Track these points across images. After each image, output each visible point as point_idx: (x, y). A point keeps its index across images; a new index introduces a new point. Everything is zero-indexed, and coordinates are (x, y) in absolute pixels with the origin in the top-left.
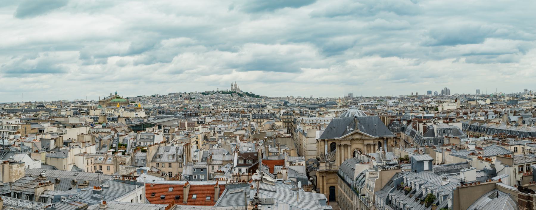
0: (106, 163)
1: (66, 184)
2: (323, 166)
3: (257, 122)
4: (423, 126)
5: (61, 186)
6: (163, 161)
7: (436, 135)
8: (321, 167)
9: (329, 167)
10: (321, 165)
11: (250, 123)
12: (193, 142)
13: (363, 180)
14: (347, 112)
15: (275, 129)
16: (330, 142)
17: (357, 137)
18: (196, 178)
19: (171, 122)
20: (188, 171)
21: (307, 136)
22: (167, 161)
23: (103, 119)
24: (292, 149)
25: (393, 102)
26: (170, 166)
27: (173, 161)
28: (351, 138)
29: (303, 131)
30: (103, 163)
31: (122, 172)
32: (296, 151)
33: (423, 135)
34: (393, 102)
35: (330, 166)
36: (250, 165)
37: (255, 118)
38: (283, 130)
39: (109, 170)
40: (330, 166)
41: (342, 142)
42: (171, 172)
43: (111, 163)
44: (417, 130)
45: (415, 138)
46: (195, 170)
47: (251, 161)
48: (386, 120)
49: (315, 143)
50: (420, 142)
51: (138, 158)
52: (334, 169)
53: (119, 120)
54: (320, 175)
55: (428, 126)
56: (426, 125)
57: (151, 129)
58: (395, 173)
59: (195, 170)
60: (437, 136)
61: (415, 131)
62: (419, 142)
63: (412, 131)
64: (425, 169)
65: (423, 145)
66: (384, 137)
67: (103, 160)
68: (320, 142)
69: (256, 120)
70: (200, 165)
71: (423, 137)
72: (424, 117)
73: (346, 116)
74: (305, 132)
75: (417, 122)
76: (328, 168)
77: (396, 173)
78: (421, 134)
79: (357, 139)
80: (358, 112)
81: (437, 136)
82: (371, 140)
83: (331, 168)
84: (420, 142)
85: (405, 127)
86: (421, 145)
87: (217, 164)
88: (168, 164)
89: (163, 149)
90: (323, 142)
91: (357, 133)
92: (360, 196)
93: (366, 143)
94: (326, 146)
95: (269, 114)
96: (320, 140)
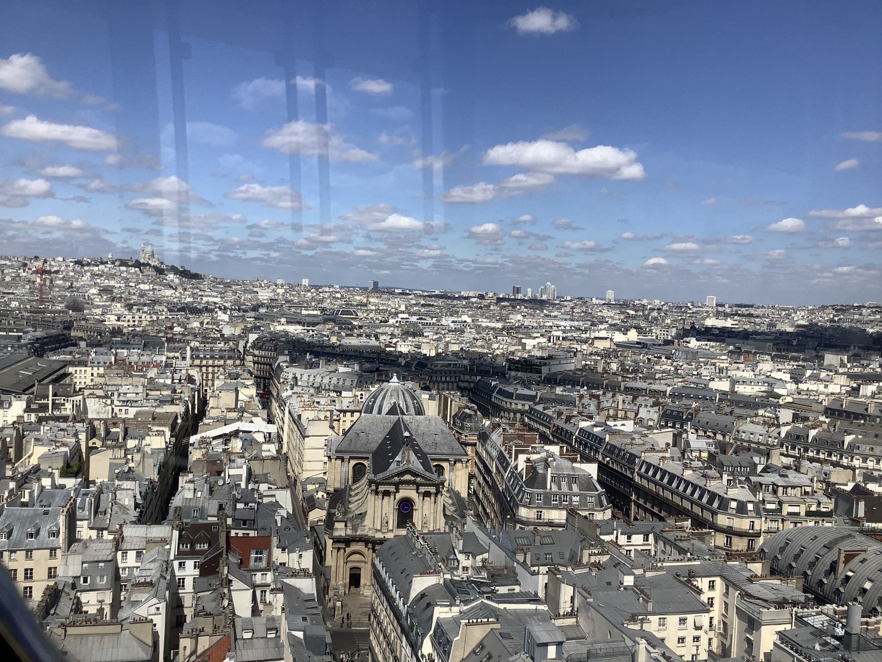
2: (341, 529)
7: (548, 487)
8: (337, 529)
10: (338, 525)
16: (353, 462)
17: (408, 477)
18: (89, 582)
20: (71, 567)
21: (307, 434)
25: (453, 322)
29: (299, 416)
33: (524, 480)
34: (453, 322)
35: (355, 528)
40: (355, 528)
42: (31, 570)
44: (510, 457)
49: (321, 447)
52: (362, 533)
60: (551, 489)
61: (507, 456)
64: (549, 657)
68: (333, 461)
72: (517, 394)
74: (304, 420)
76: (349, 532)
77: (491, 629)
79: (408, 482)
81: (551, 489)
87: (133, 548)
91: (408, 472)
93: (422, 489)
95: (225, 350)
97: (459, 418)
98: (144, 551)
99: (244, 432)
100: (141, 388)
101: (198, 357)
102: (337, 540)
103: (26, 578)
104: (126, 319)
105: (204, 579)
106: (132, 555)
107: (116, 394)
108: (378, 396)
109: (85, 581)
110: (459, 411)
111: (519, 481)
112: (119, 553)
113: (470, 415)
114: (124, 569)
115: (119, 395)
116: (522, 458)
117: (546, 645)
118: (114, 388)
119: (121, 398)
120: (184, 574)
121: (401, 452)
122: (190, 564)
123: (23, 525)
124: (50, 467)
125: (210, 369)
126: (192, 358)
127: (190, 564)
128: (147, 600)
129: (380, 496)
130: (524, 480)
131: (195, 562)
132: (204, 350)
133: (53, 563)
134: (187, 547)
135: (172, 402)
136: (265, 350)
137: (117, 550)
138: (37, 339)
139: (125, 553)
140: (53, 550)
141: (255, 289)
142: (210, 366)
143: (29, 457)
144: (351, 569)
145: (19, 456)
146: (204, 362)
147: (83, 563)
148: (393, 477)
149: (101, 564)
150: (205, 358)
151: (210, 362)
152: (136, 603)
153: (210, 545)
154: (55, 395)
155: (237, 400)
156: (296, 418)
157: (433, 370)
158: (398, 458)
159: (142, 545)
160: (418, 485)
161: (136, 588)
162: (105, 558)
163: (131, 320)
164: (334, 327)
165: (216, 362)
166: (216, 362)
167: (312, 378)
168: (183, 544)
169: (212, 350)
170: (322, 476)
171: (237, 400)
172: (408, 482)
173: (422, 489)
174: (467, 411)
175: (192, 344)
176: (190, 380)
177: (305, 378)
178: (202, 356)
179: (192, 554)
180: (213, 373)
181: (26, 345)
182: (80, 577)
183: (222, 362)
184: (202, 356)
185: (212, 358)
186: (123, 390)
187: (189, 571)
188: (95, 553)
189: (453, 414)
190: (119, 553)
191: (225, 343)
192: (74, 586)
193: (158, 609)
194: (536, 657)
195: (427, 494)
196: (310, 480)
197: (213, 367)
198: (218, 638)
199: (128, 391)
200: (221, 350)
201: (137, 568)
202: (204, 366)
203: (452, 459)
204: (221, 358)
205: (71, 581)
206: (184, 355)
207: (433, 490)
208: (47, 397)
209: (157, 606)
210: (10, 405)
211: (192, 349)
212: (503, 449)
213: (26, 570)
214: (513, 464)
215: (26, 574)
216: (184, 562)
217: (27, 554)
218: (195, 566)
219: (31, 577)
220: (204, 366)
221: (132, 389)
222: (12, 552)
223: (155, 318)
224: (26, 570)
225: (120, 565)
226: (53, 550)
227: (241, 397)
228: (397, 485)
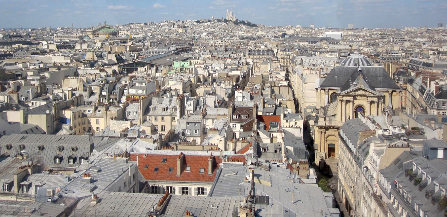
0: (95, 116)
1: (51, 151)
3: (253, 59)
4: (436, 86)
5: (46, 153)
6: (156, 114)
9: (329, 122)
11: (246, 61)
12: (187, 87)
13: (366, 151)
14: (349, 58)
15: (272, 72)
16: (331, 92)
19: (164, 59)
20: (182, 125)
22: (160, 114)
24: (290, 100)
26: (163, 118)
27: (166, 114)
28: (353, 93)
29: (302, 75)
30: (92, 116)
31: (113, 127)
32: (293, 102)
33: (434, 95)
36: (245, 121)
37: (251, 55)
38: (281, 73)
39: (99, 123)
40: (330, 121)
41: (344, 97)
42: (164, 126)
43: (101, 116)
44: (427, 87)
45: (424, 95)
46: (188, 125)
47: (246, 118)
48: (391, 67)
50: (431, 103)
51: (130, 111)
54: (319, 131)
55: (442, 86)
56: (438, 84)
57: (143, 69)
58: (403, 151)
59: (188, 125)
61: (424, 86)
62: (429, 103)
63: (422, 86)
65: (434, 107)
66: (389, 91)
68: (319, 91)
69: (251, 57)
71: (434, 98)
73: (346, 65)
75: (428, 79)
78: (432, 94)
79: (361, 95)
80: (361, 58)
82: (375, 97)
83: (331, 124)
84: (431, 103)
85: (414, 79)
86: (432, 106)
88: (161, 117)
89: (156, 100)
90: (322, 91)
91: (360, 89)
92: (362, 168)
93: (370, 99)
94: (326, 96)
95: (265, 51)
96: (320, 89)
97: (397, 75)
100: (222, 64)
102: (320, 128)
103: (162, 130)
104: (219, 43)
105: (246, 133)
108: (347, 60)
109: (188, 132)
110: (397, 71)
111: (431, 96)
113: (403, 72)
115: (212, 68)
116: (433, 83)
117: (436, 149)
119: (213, 69)
120: (236, 131)
121: (356, 80)
122: (238, 125)
127: (238, 125)
129: (344, 103)
130: (434, 95)
131: (241, 125)
135: (237, 70)
144: (329, 145)
145: (164, 85)
148: (351, 92)
151: (258, 57)
153: (248, 116)
156: (301, 76)
157: (383, 58)
158: (354, 83)
160: (367, 97)
163: (221, 43)
169: (259, 51)
170: (315, 105)
172: (361, 95)
173: (370, 99)
174: (401, 70)
176: (247, 64)
177: (307, 61)
179: (240, 121)
185: (259, 54)
187: (238, 129)
188: (193, 120)
189: (393, 73)
192: (184, 134)
194: (429, 157)
195: (372, 102)
196: (308, 108)
198: (247, 144)
202: (255, 59)
203: (390, 90)
205: (182, 131)
207: (376, 99)
212: (423, 84)
213: (162, 126)
214: (428, 89)
215: (162, 128)
216: (235, 125)
218: (241, 127)
219: (165, 130)
220: (255, 59)
221: (218, 65)
223: (232, 41)
224: (162, 126)
228: (355, 97)
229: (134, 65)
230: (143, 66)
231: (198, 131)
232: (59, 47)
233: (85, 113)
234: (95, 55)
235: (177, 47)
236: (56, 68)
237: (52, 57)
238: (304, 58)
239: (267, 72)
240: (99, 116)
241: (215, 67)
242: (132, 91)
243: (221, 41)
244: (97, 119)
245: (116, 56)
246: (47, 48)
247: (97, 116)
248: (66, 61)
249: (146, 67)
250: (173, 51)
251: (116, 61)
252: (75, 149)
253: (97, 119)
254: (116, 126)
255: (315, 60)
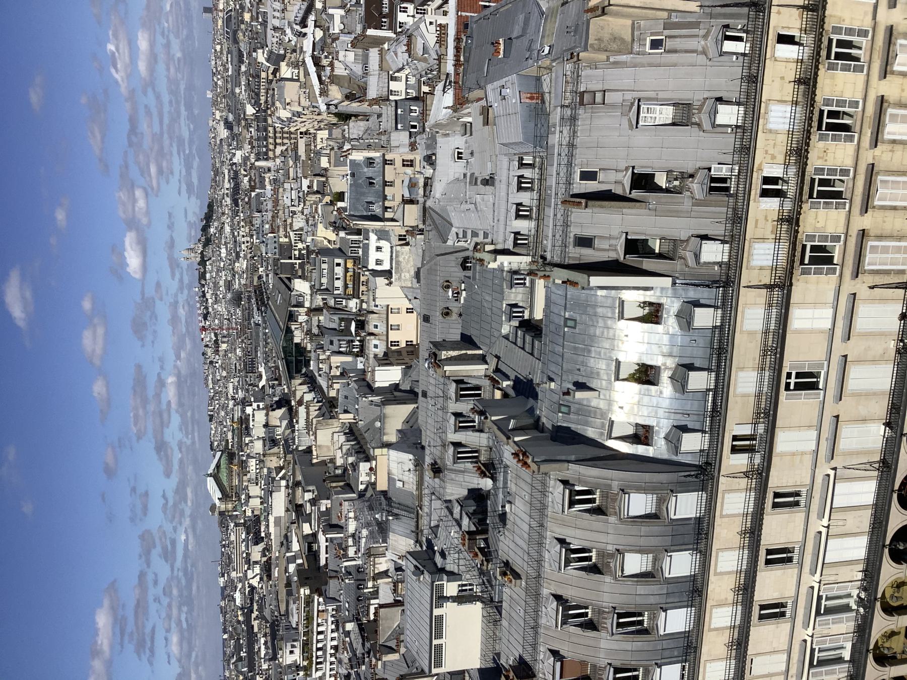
0: (385, 333)
18: (415, 124)
22: (381, 189)
23: (272, 458)
30: (385, 338)
39: (399, 325)
43: (385, 322)
53: (274, 424)
67: (379, 340)
70: (390, 121)
95: (258, 125)
98: (391, 72)
99: (314, 50)
101: (266, 153)
106: (394, 85)
107: (292, 209)
112: (392, 98)
114: (407, 93)
118: (287, 210)
119: (296, 203)
123: (363, 194)
124: (332, 213)
125: (278, 141)
126: (267, 159)
128: (423, 37)
131: (400, 11)
132: (258, 147)
133: (399, 163)
134: (385, 22)
136: (259, 89)
137: (388, 100)
138: (258, 309)
139: (391, 92)
140: (385, 162)
141: (218, 142)
142: (275, 141)
143: (329, 241)
146: (271, 147)
147: (396, 128)
149: (399, 111)
150: (266, 146)
151: (271, 141)
152: (425, 50)
154: (290, 258)
155: (291, 80)
159: (384, 75)
161: (412, 53)
162: (393, 109)
163: (246, 245)
164: (242, 30)
165: (271, 135)
166: (271, 135)
167: (277, 14)
168: (382, 26)
169: (258, 139)
171: (291, 80)
175: (253, 160)
178: (264, 149)
180: (283, 138)
181: (263, 317)
182: (410, 132)
183: (271, 129)
184: (264, 149)
185: (266, 138)
186: (288, 202)
190: (392, 98)
191: (251, 126)
193: (431, 23)
197: (275, 138)
199: (289, 198)
200: (258, 130)
201: (407, 81)
204: (266, 130)
206: (266, 170)
208: (293, 264)
209: (428, 24)
210: (300, 295)
211: (258, 160)
216: (400, 23)
217: (389, 186)
221: (287, 194)
222: (385, 198)
225: (403, 97)
226: (385, 162)
227: (288, 76)
229: (289, 358)
230: (292, 332)
231: (412, 123)
232: (258, 540)
233: (381, 355)
234: (272, 451)
235: (255, 309)
236: (296, 489)
237: (275, 518)
238: (270, 26)
239: (299, 72)
240: (385, 325)
241: (292, 200)
242: (337, 288)
243: (243, 245)
244: (391, 329)
245: (273, 410)
246: (258, 566)
247: (385, 329)
248: (283, 489)
249: (293, 327)
250: (262, 314)
251: (283, 409)
252: (446, 284)
253: (391, 329)
254: (403, 275)
255: (274, 6)
